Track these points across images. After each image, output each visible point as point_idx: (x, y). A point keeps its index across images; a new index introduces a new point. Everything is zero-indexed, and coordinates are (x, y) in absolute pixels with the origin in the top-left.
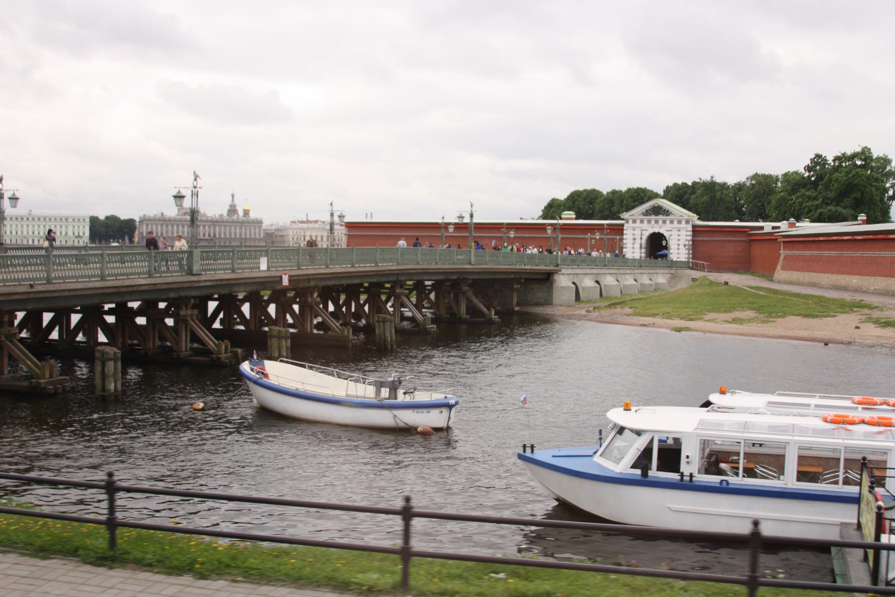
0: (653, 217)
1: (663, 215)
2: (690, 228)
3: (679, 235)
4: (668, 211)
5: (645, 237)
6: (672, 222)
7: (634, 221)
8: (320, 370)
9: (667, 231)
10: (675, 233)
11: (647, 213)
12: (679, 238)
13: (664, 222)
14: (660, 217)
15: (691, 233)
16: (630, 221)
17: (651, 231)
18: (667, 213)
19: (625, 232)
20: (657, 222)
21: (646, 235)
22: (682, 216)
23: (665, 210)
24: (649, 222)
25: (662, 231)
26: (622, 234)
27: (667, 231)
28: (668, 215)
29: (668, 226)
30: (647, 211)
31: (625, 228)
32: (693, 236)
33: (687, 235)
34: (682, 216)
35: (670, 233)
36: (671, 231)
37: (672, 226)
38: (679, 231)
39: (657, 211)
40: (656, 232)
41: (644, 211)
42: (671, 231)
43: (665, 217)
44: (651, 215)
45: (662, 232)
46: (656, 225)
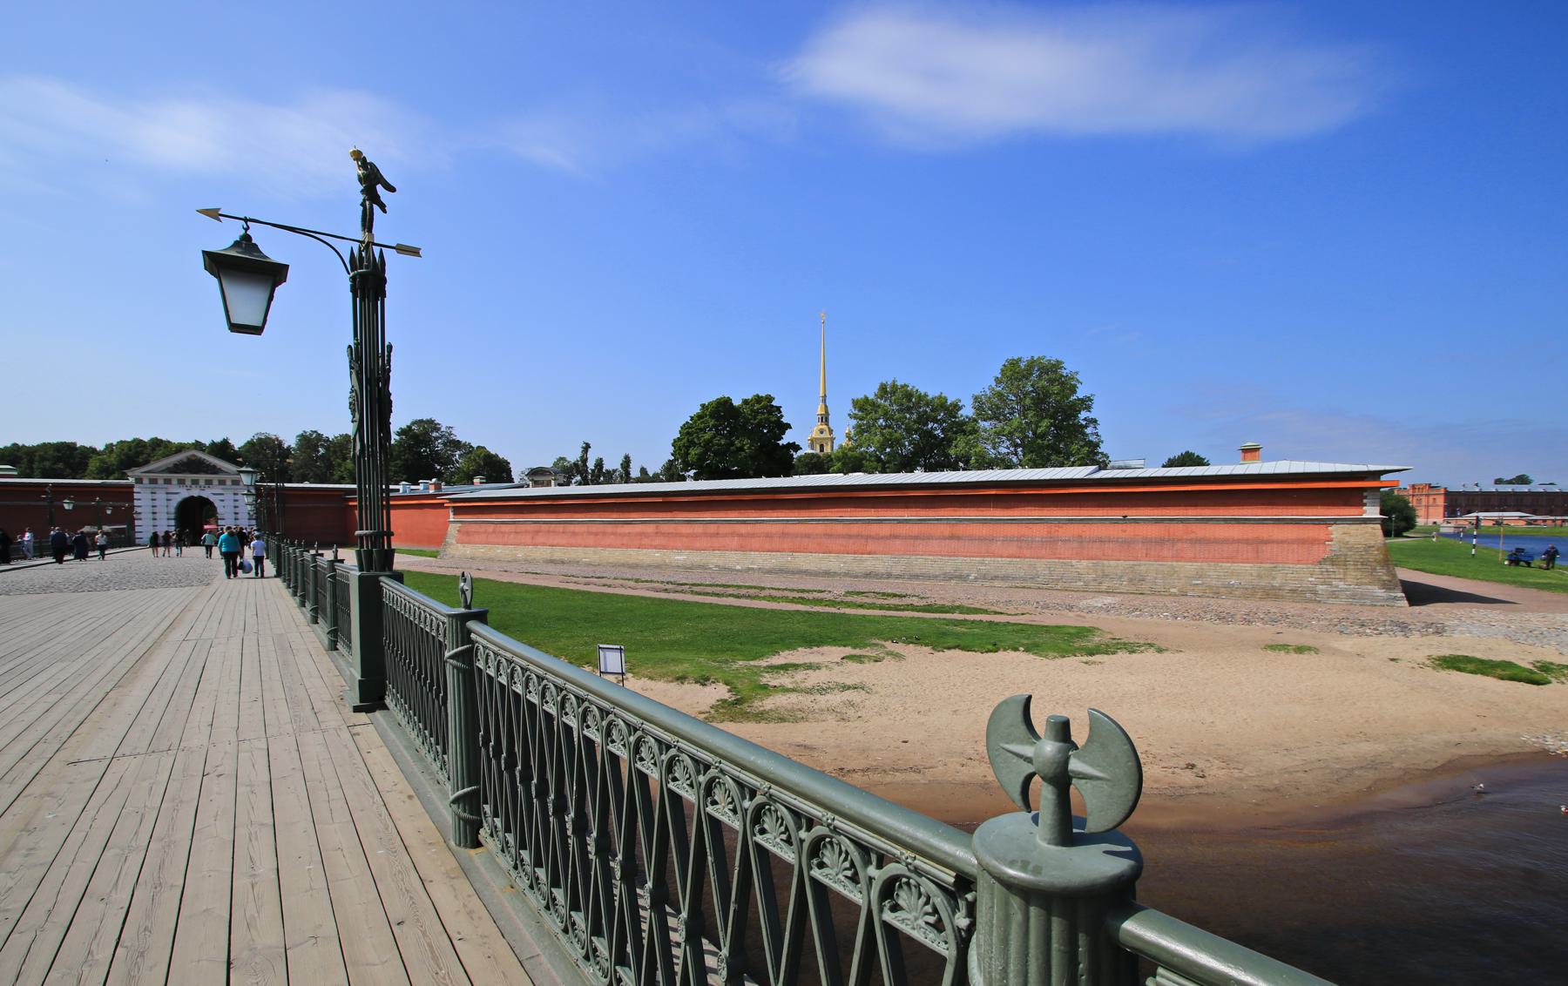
0: (189, 477)
1: (207, 473)
6: (222, 482)
7: (153, 481)
8: (1499, 671)
9: (214, 494)
10: (229, 496)
11: (176, 469)
12: (237, 504)
13: (209, 482)
14: (202, 477)
16: (146, 481)
17: (184, 493)
18: (215, 470)
19: (136, 496)
20: (195, 482)
21: (177, 499)
24: (181, 482)
26: (132, 500)
27: (214, 494)
30: (175, 465)
31: (135, 490)
35: (221, 497)
39: (195, 466)
41: (171, 466)
43: (209, 477)
46: (193, 486)
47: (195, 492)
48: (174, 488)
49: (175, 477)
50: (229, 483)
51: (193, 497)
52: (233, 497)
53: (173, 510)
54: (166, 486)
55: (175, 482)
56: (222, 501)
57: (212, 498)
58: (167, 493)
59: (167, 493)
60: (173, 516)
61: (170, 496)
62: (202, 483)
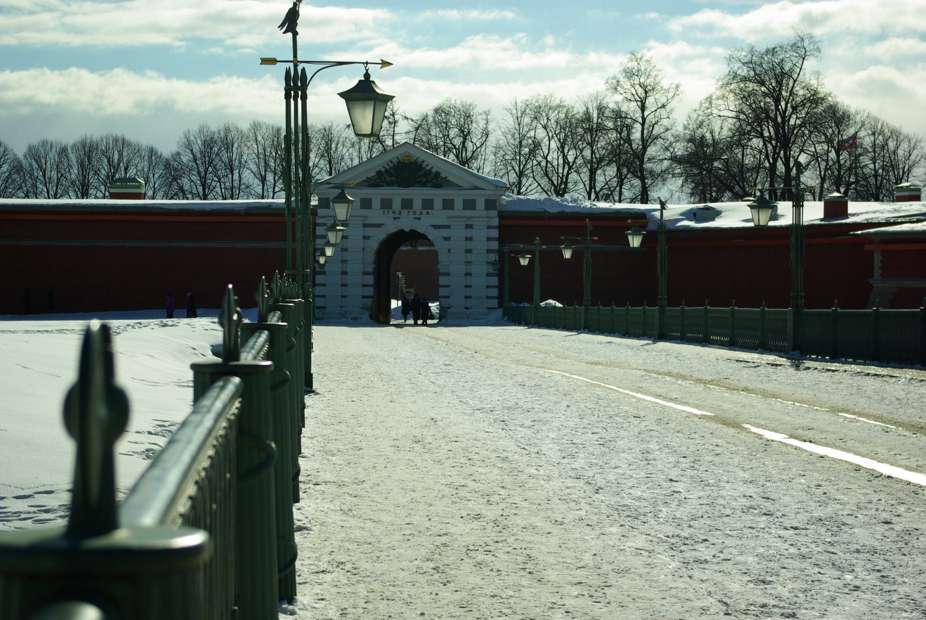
0: (397, 194)
1: (423, 185)
2: (496, 222)
3: (469, 239)
4: (438, 174)
5: (374, 245)
6: (448, 204)
12: (469, 245)
13: (428, 204)
14: (417, 194)
15: (495, 233)
20: (407, 204)
21: (379, 236)
22: (476, 188)
23: (430, 171)
24: (386, 204)
25: (421, 227)
27: (436, 227)
28: (438, 186)
29: (439, 216)
30: (379, 173)
32: (502, 240)
33: (489, 239)
34: (476, 188)
35: (445, 232)
36: (448, 227)
37: (449, 213)
38: (469, 227)
40: (407, 229)
41: (372, 174)
42: (448, 227)
43: (428, 192)
44: (390, 184)
45: (420, 230)
46: (405, 212)
47: (406, 224)
48: (375, 214)
49: (377, 194)
50: (459, 204)
51: (403, 231)
52: (463, 233)
53: (371, 258)
54: (364, 212)
55: (376, 203)
56: (447, 239)
57: (432, 234)
58: (365, 226)
59: (365, 226)
60: (370, 268)
61: (370, 231)
62: (417, 205)
